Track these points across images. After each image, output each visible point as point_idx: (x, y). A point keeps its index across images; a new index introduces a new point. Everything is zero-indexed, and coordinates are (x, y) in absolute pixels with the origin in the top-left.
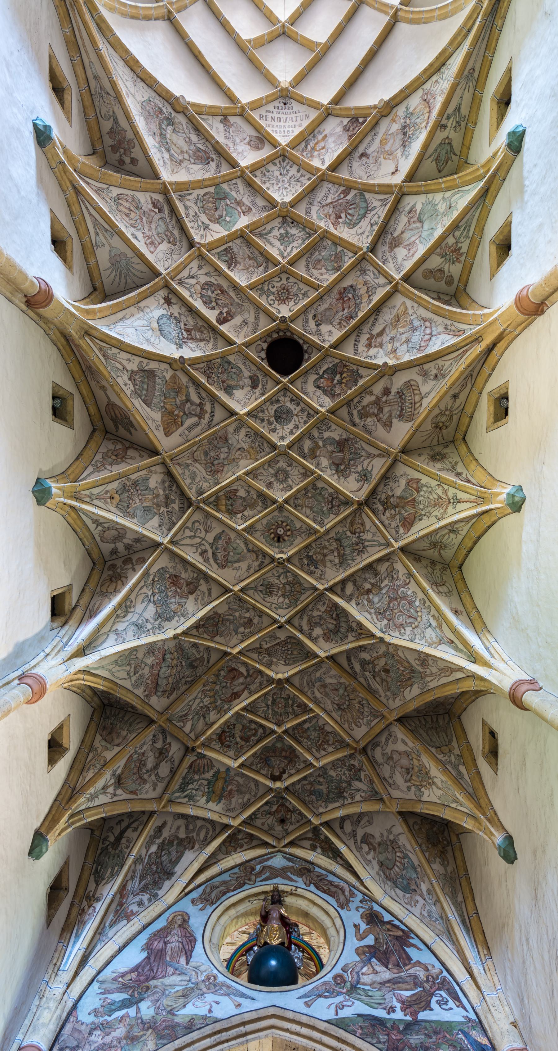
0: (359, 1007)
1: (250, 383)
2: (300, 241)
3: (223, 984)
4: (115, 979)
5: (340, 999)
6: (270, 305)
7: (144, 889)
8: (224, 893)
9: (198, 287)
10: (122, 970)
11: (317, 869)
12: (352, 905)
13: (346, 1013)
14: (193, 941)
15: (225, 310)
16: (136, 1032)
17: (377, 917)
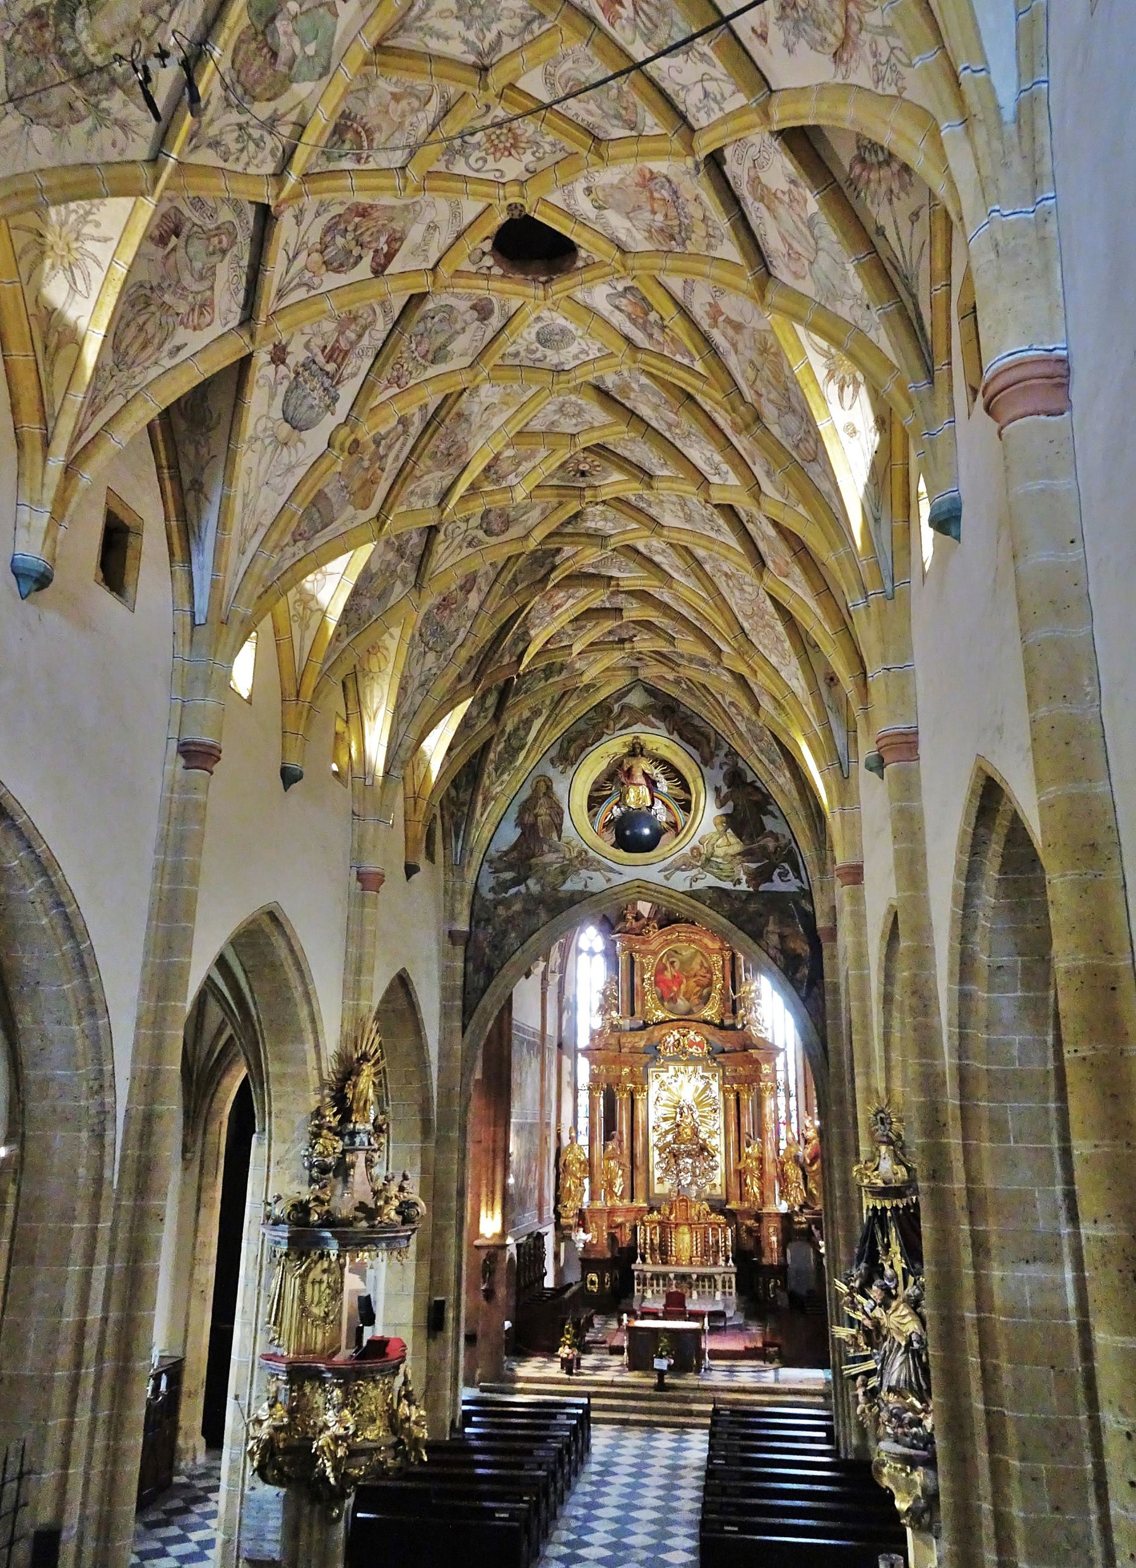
0: (710, 880)
1: (476, 314)
2: (519, 23)
3: (594, 860)
4: (500, 858)
5: (694, 872)
6: (477, 171)
7: (502, 773)
8: (583, 749)
9: (316, 256)
10: (505, 849)
11: (682, 709)
12: (717, 761)
13: (699, 885)
14: (560, 813)
15: (383, 239)
16: (531, 906)
17: (740, 776)
